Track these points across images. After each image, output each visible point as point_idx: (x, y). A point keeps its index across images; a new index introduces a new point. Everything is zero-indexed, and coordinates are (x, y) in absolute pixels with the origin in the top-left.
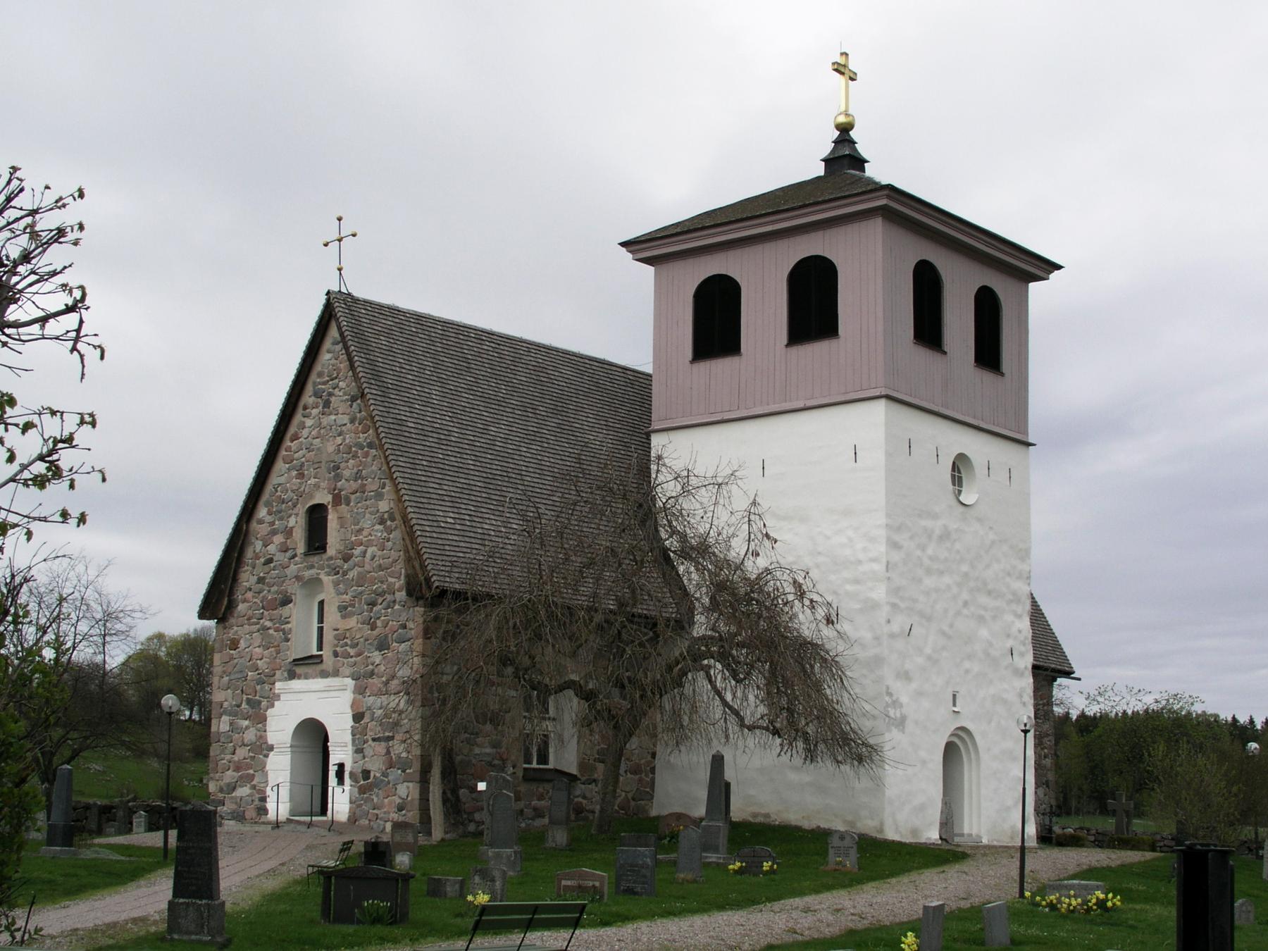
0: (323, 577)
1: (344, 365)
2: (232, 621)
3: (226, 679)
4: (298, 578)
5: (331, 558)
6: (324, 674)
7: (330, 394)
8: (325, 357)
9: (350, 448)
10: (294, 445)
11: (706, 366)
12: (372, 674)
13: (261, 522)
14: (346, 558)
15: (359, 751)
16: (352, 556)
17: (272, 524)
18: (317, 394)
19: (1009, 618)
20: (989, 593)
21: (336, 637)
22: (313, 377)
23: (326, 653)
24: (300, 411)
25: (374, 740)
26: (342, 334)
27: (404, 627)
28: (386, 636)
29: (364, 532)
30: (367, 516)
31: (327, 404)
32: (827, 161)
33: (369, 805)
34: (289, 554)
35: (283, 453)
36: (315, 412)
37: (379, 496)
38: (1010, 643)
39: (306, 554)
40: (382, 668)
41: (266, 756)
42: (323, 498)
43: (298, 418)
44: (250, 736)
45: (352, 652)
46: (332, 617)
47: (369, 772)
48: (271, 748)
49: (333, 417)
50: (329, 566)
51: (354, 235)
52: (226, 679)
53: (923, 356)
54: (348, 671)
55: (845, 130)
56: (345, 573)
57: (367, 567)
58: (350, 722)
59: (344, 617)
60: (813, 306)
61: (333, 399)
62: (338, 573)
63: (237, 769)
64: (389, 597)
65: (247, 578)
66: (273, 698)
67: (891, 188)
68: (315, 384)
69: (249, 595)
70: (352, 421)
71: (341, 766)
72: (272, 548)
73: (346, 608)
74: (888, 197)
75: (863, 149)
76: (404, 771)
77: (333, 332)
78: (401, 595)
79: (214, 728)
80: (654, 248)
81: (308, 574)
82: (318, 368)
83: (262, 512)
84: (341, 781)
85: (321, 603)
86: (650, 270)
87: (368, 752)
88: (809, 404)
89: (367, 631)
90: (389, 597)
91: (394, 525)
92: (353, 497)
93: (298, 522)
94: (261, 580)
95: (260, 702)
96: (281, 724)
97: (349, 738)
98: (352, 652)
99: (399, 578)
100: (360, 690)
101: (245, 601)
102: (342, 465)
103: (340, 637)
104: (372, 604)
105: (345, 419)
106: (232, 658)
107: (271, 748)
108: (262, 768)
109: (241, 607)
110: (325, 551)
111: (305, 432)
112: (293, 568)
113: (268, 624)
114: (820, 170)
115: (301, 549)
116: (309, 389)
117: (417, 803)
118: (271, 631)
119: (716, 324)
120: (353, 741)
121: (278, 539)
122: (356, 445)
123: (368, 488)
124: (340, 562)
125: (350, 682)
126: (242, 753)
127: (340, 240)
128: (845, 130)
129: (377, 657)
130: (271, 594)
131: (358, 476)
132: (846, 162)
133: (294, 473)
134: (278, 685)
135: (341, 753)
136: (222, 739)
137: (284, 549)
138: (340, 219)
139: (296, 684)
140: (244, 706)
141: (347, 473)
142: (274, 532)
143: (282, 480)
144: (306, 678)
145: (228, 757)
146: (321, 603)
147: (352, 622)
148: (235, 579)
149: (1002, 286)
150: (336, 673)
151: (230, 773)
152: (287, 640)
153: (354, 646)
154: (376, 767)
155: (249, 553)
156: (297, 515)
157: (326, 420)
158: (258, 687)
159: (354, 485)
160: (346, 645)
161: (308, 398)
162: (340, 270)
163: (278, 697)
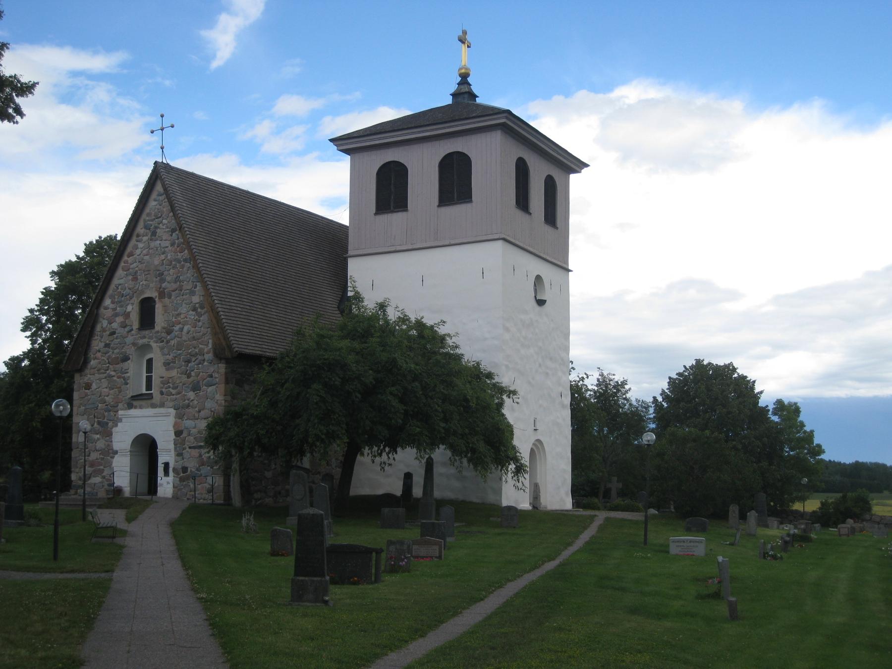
0: (154, 345)
1: (166, 208)
2: (87, 371)
3: (83, 408)
4: (134, 344)
5: (158, 332)
6: (154, 406)
7: (156, 228)
8: (152, 204)
10: (130, 260)
11: (385, 218)
12: (188, 406)
13: (106, 308)
14: (169, 332)
15: (179, 454)
17: (115, 309)
18: (147, 227)
19: (560, 374)
20: (551, 359)
21: (162, 383)
22: (144, 216)
23: (155, 391)
24: (134, 238)
25: (190, 448)
26: (165, 189)
27: (211, 376)
28: (198, 382)
29: (184, 314)
30: (184, 305)
31: (154, 234)
32: (454, 95)
34: (127, 329)
35: (122, 264)
36: (145, 238)
37: (192, 293)
38: (561, 389)
40: (195, 402)
41: (113, 457)
42: (154, 294)
43: (133, 242)
44: (101, 444)
45: (174, 392)
46: (159, 371)
47: (187, 468)
48: (116, 452)
49: (158, 242)
51: (172, 126)
52: (83, 408)
53: (519, 214)
54: (171, 404)
55: (464, 78)
56: (168, 342)
57: (184, 338)
58: (173, 436)
59: (167, 370)
60: (455, 181)
61: (158, 231)
62: (163, 341)
63: (92, 465)
64: (200, 358)
65: (97, 344)
66: (116, 421)
67: (509, 112)
68: (145, 221)
69: (99, 355)
70: (173, 244)
71: (166, 465)
73: (169, 364)
74: (507, 118)
75: (475, 89)
76: (212, 468)
77: (159, 187)
78: (209, 356)
79: (74, 440)
80: (348, 144)
81: (141, 342)
82: (147, 210)
84: (166, 473)
85: (150, 362)
86: (348, 158)
87: (186, 455)
88: (453, 242)
89: (184, 378)
90: (200, 358)
91: (203, 311)
92: (173, 293)
93: (133, 309)
94: (107, 346)
95: (107, 424)
96: (123, 436)
97: (172, 446)
98: (174, 392)
99: (207, 345)
100: (180, 416)
101: (95, 358)
102: (166, 273)
103: (165, 382)
104: (189, 361)
105: (168, 243)
106: (86, 395)
107: (116, 452)
108: (109, 465)
109: (93, 363)
110: (154, 328)
111: (138, 252)
112: (129, 340)
113: (113, 373)
114: (449, 101)
115: (136, 325)
116: (141, 224)
117: (221, 488)
118: (115, 378)
120: (175, 448)
121: (119, 319)
122: (175, 260)
123: (184, 288)
124: (164, 335)
125: (172, 411)
126: (94, 456)
127: (162, 129)
128: (464, 78)
129: (191, 395)
130: (115, 353)
131: (177, 280)
132: (466, 96)
133: (130, 277)
134: (120, 412)
135: (166, 455)
137: (124, 325)
138: (162, 116)
139: (133, 412)
141: (168, 278)
142: (116, 315)
143: (121, 281)
144: (141, 407)
146: (150, 362)
147: (174, 373)
148: (89, 345)
149: (556, 174)
150: (162, 405)
152: (127, 384)
153: (175, 388)
154: (192, 465)
155: (98, 328)
156: (133, 304)
157: (152, 244)
158: (106, 414)
159: (174, 286)
160: (169, 387)
161: (140, 229)
162: (162, 148)
163: (120, 420)
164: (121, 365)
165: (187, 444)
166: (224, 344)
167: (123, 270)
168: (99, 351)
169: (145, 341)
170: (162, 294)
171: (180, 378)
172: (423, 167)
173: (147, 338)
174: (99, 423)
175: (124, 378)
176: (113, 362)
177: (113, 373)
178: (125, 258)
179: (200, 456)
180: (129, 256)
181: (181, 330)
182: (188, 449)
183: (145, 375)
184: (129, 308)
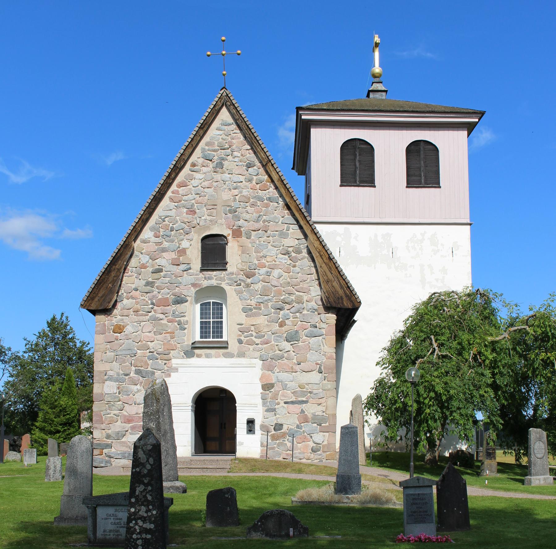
0: (227, 288)
5: (232, 274)
6: (226, 356)
9: (249, 199)
10: (181, 190)
12: (282, 357)
16: (254, 275)
25: (285, 403)
31: (220, 165)
33: (282, 448)
34: (183, 267)
35: (169, 194)
37: (283, 235)
39: (202, 270)
45: (258, 341)
47: (282, 425)
50: (230, 279)
54: (258, 354)
56: (248, 286)
60: (423, 167)
61: (226, 163)
65: (131, 281)
68: (203, 150)
71: (251, 422)
72: (164, 261)
81: (206, 284)
82: (206, 139)
83: (147, 233)
89: (276, 327)
94: (148, 284)
95: (153, 373)
98: (258, 341)
111: (194, 183)
112: (187, 279)
115: (197, 264)
118: (164, 322)
119: (358, 166)
120: (264, 404)
129: (287, 346)
134: (175, 362)
136: (107, 398)
139: (194, 361)
140: (132, 374)
142: (164, 250)
144: (207, 356)
145: (117, 412)
147: (261, 320)
150: (241, 355)
151: (119, 423)
154: (290, 422)
157: (218, 177)
163: (176, 370)
164: (171, 309)
165: (281, 400)
166: (341, 292)
167: (171, 199)
168: (136, 290)
169: (214, 282)
170: (237, 233)
171: (267, 325)
172: (390, 149)
173: (214, 278)
174: (138, 372)
175: (179, 323)
176: (164, 303)
177: (162, 316)
178: (174, 187)
179: (302, 412)
180: (179, 186)
181: (268, 274)
182: (282, 404)
183: (224, 320)
184: (185, 244)
